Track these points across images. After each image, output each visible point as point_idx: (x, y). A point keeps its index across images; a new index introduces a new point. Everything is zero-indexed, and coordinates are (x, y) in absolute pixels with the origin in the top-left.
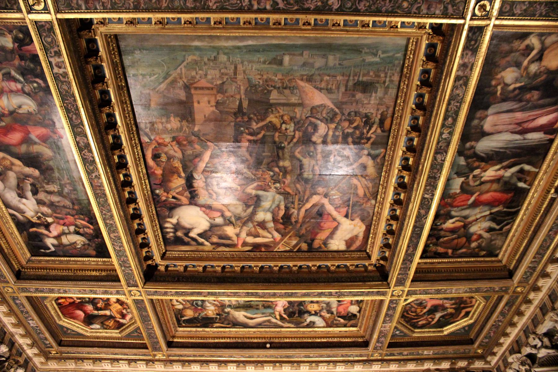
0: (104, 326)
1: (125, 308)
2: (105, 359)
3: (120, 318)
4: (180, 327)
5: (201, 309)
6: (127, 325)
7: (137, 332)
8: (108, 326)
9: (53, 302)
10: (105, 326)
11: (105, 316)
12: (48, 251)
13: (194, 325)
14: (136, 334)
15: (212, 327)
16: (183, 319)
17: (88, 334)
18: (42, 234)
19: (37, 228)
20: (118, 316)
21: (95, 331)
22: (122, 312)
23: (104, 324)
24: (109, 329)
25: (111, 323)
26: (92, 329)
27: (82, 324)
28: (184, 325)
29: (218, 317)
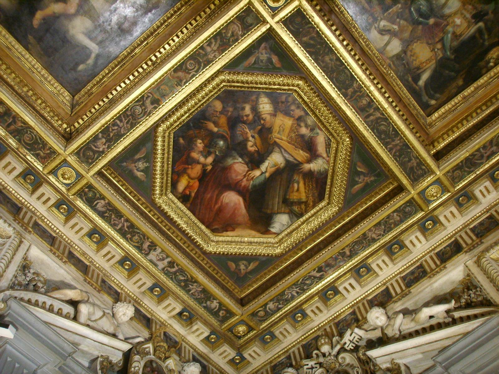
0: (297, 211)
1: (299, 119)
2: (339, 278)
3: (309, 161)
4: (429, 115)
5: (436, 24)
6: (330, 174)
7: (359, 174)
8: (300, 203)
9: (171, 196)
10: (296, 208)
11: (278, 173)
12: (91, 61)
13: (453, 88)
14: (361, 181)
15: (489, 69)
16: (421, 83)
17: (278, 251)
18: (56, 17)
19: (42, 9)
20: (301, 155)
21: (285, 233)
22: (302, 136)
23: (292, 203)
24: (306, 212)
25: (300, 190)
26: (278, 234)
27: (253, 233)
28: (433, 102)
29: (481, 24)
